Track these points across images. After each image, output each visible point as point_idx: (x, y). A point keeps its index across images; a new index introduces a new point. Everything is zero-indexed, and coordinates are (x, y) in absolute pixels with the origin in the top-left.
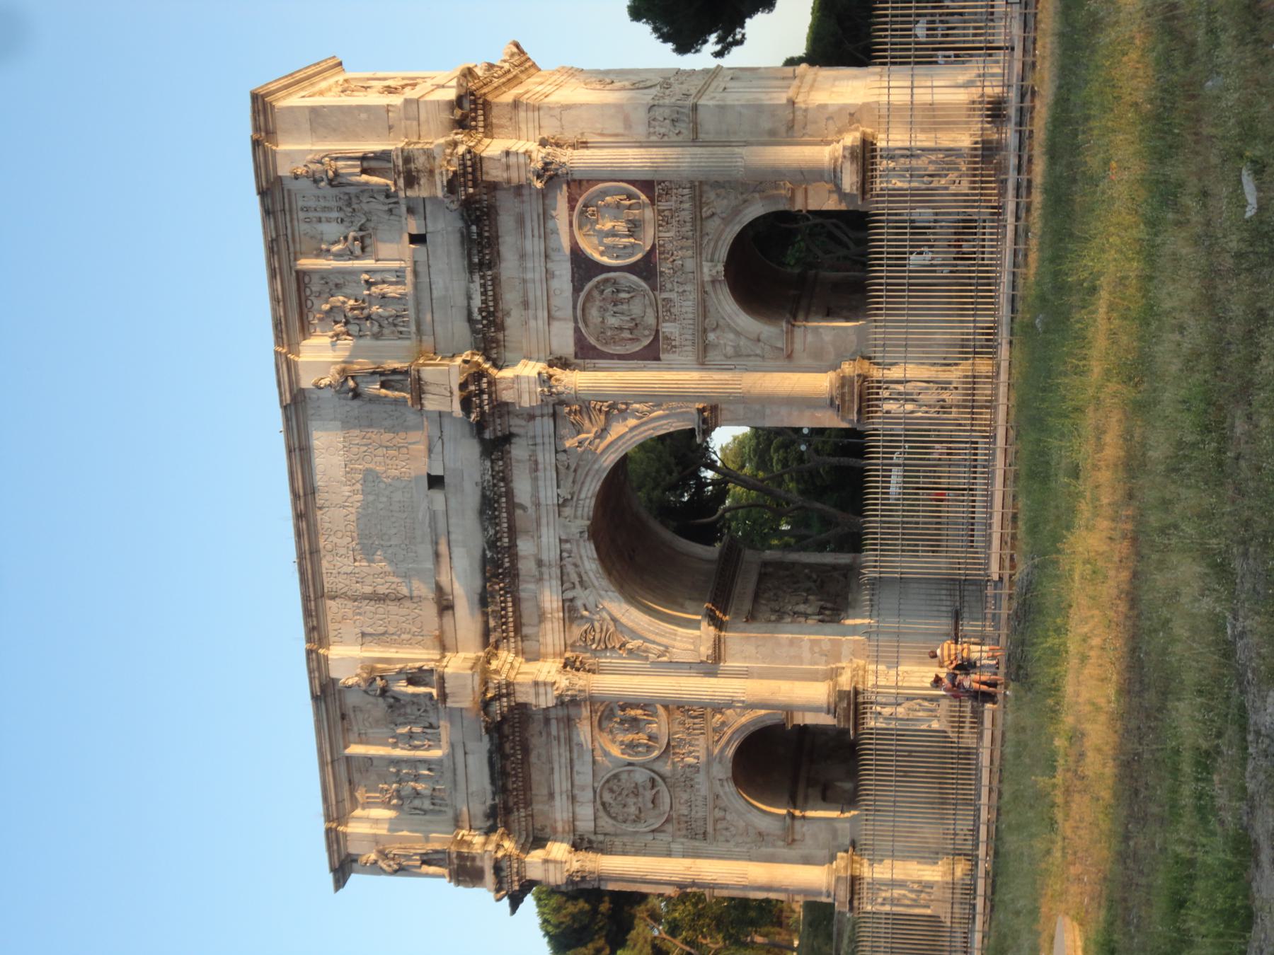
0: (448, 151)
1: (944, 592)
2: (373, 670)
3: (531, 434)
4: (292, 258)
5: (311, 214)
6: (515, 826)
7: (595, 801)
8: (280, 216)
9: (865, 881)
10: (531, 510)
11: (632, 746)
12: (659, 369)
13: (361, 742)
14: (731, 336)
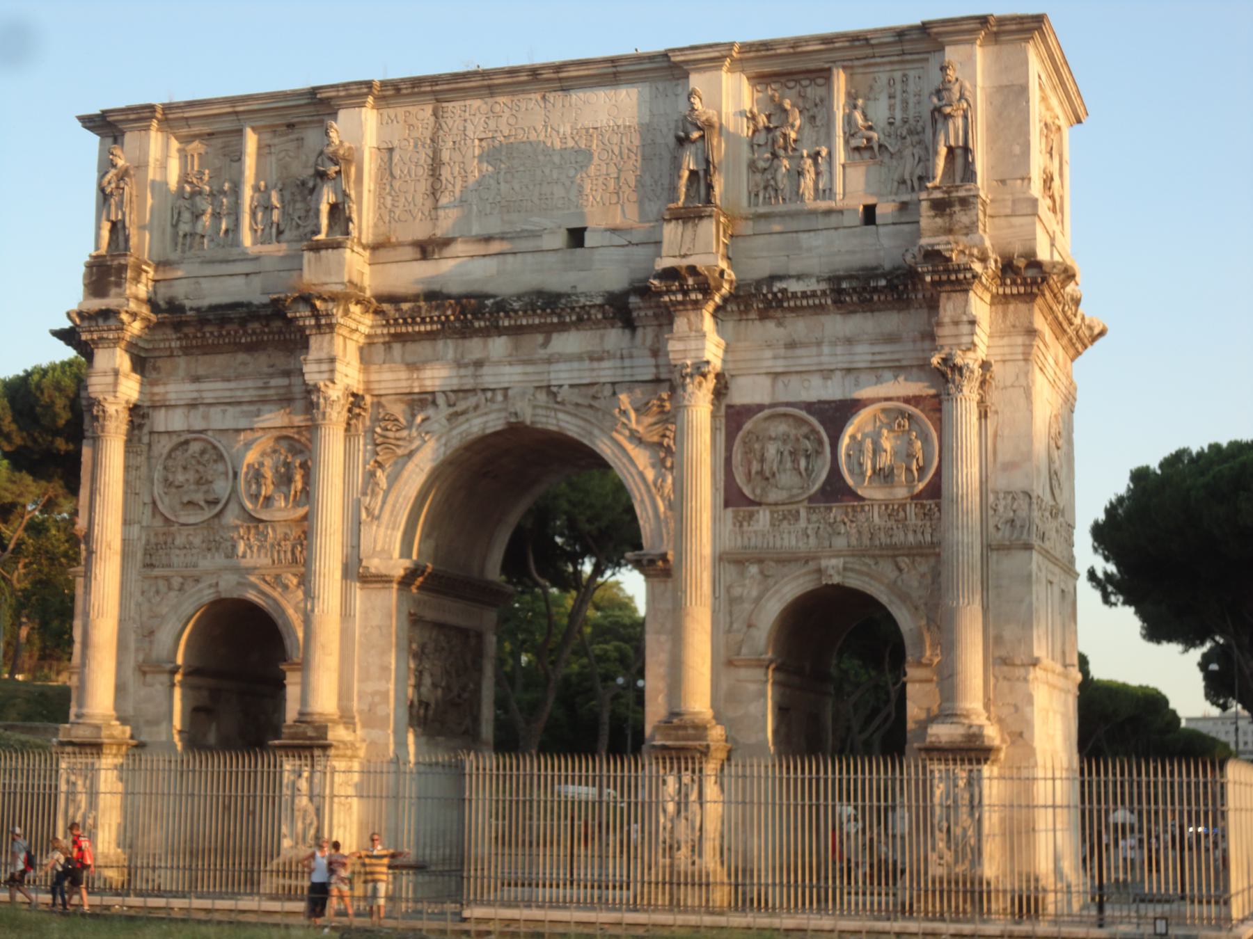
0: (975, 251)
1: (448, 851)
2: (348, 162)
3: (635, 352)
4: (845, 63)
5: (899, 87)
6: (159, 335)
7: (190, 432)
8: (898, 48)
9: (95, 760)
10: (542, 353)
11: (258, 476)
12: (714, 506)
13: (260, 148)
14: (754, 593)
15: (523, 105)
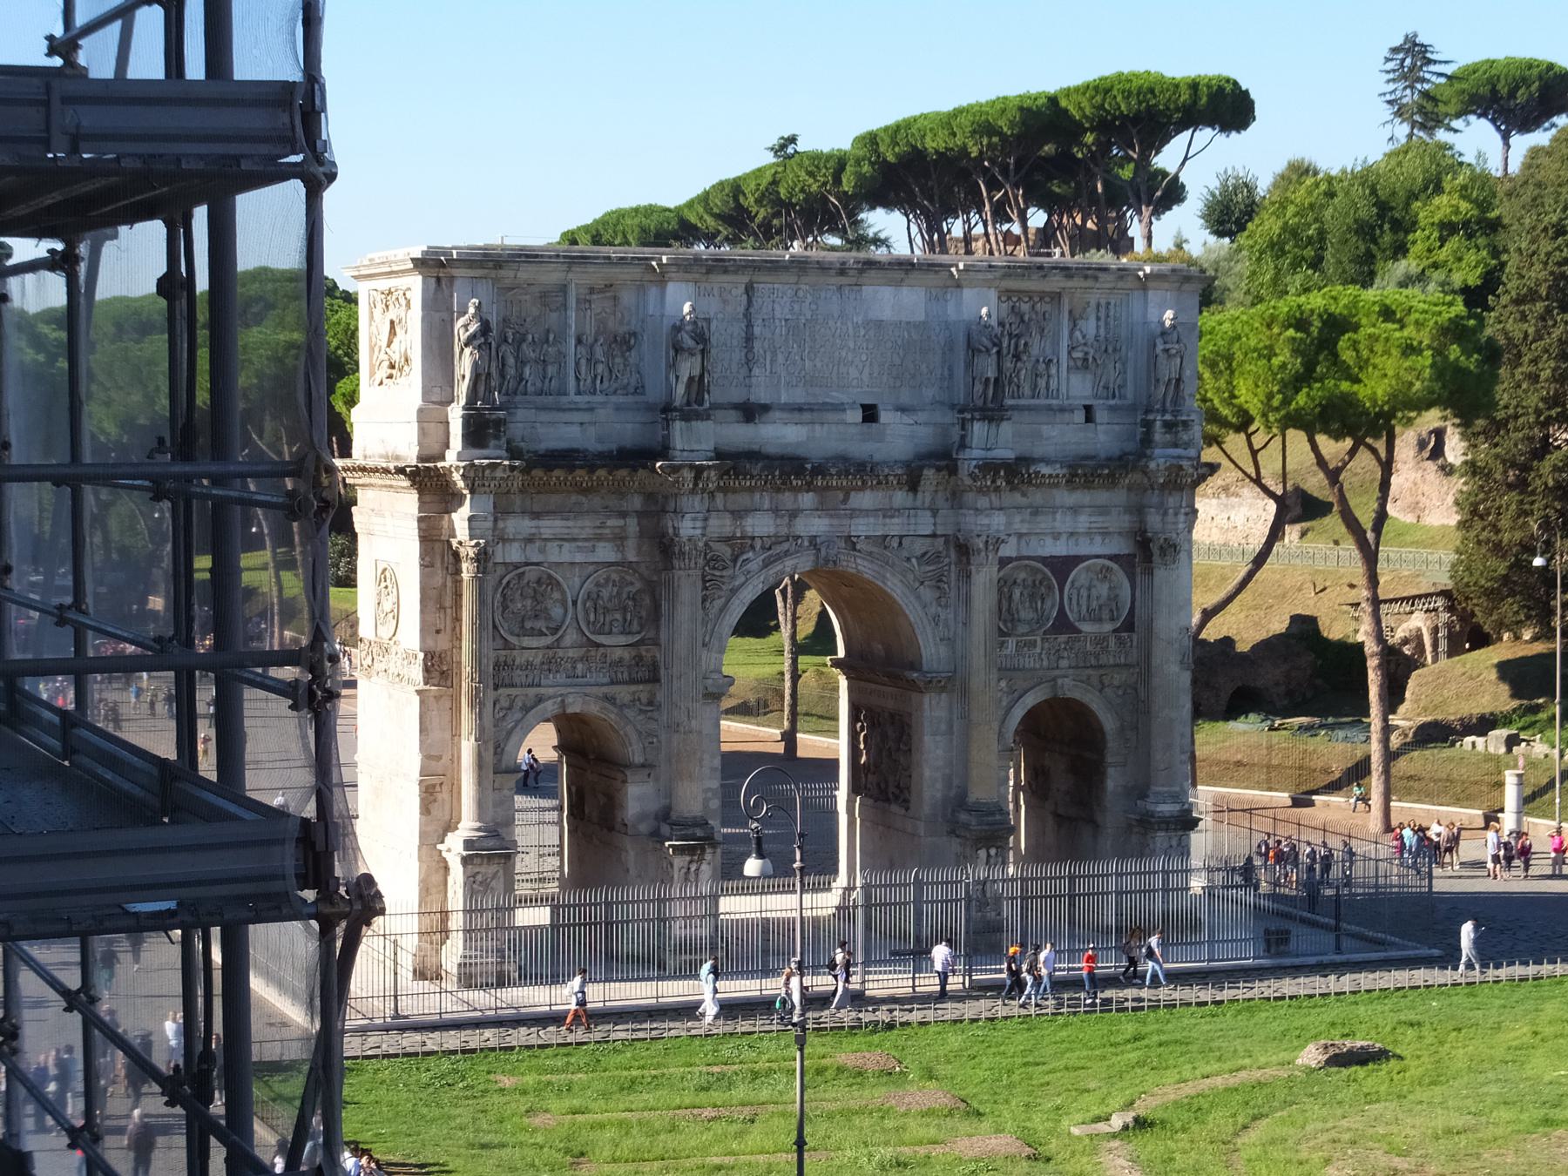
5: (1103, 310)
7: (527, 564)
14: (1004, 704)
15: (823, 295)
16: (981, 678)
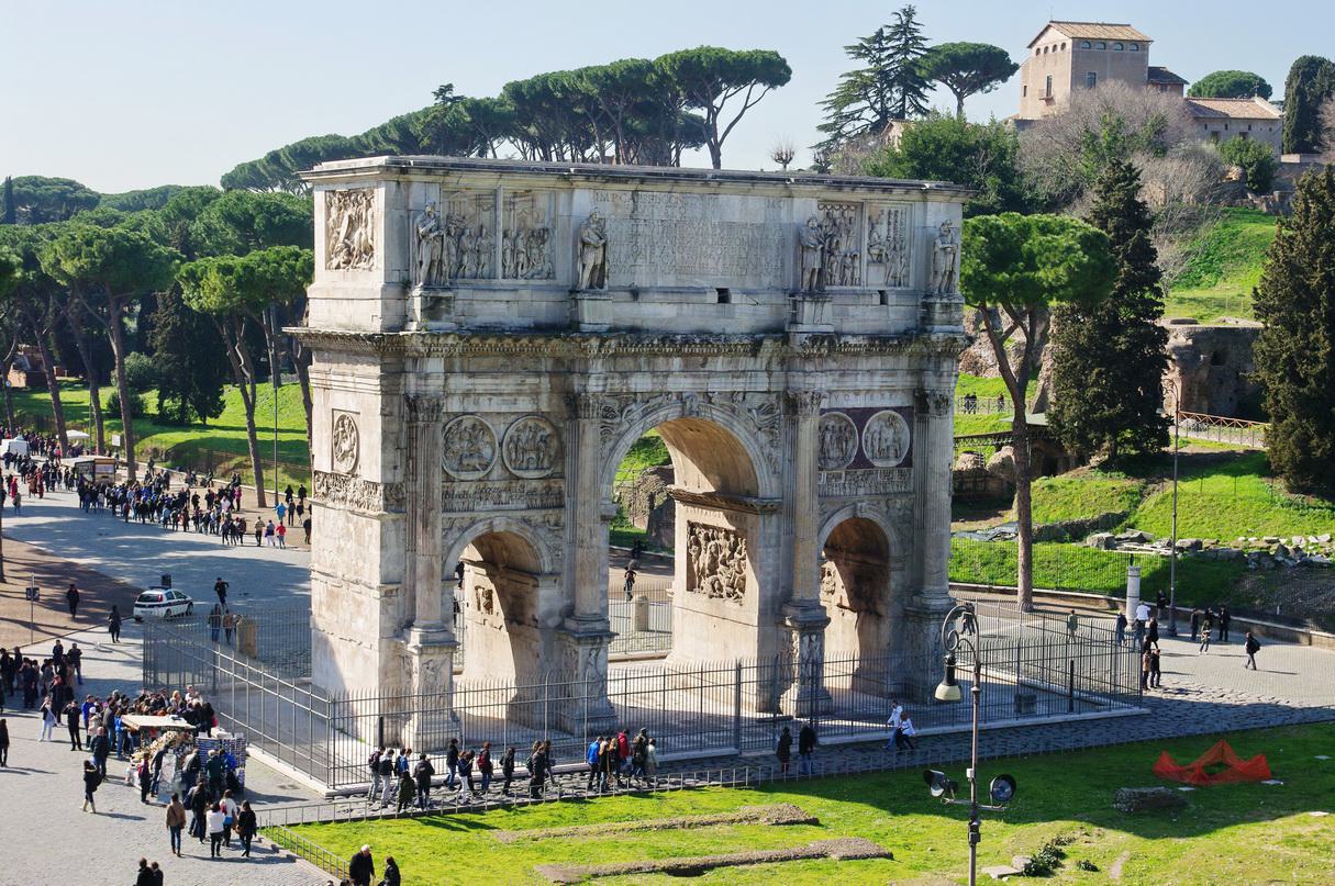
7: (464, 414)
16: (807, 505)
